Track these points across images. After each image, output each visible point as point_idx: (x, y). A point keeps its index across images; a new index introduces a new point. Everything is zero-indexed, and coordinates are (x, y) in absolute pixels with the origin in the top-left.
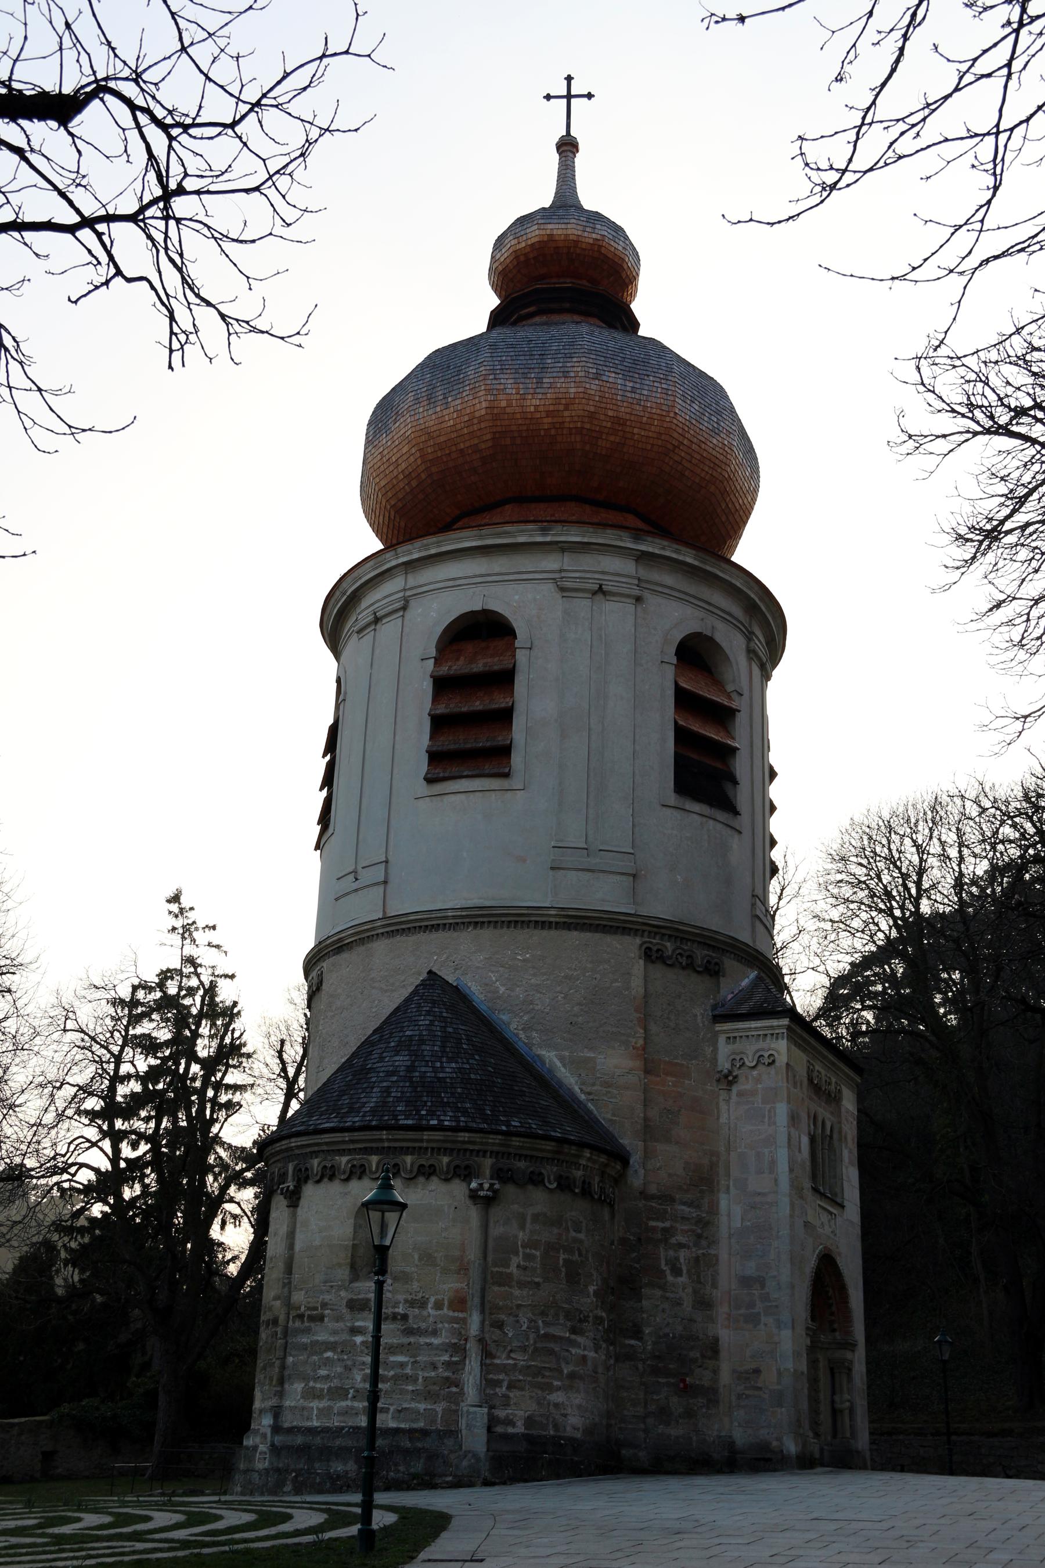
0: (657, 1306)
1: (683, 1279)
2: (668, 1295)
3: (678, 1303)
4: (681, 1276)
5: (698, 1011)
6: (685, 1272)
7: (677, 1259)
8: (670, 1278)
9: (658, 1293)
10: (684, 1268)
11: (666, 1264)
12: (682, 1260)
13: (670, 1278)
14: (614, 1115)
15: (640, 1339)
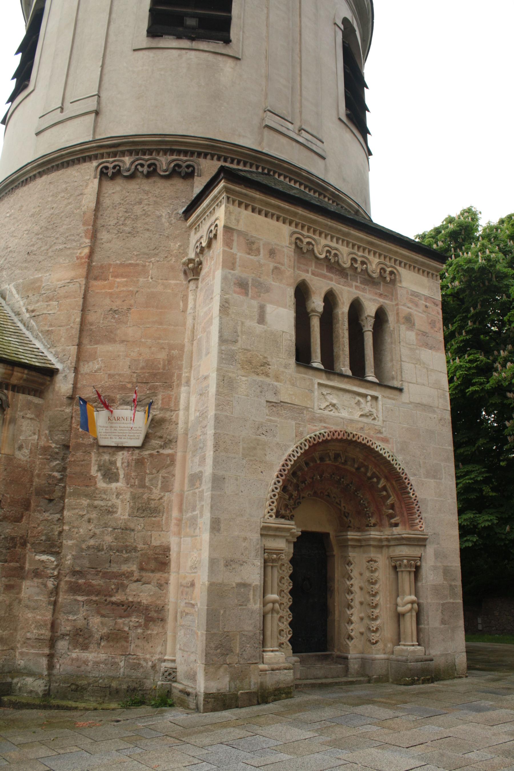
0: (82, 516)
1: (120, 484)
2: (96, 503)
3: (110, 511)
4: (117, 481)
5: (164, 212)
6: (122, 476)
7: (113, 463)
8: (101, 484)
9: (85, 502)
10: (121, 473)
11: (99, 470)
12: (119, 464)
13: (101, 484)
14: (51, 325)
15: (56, 554)
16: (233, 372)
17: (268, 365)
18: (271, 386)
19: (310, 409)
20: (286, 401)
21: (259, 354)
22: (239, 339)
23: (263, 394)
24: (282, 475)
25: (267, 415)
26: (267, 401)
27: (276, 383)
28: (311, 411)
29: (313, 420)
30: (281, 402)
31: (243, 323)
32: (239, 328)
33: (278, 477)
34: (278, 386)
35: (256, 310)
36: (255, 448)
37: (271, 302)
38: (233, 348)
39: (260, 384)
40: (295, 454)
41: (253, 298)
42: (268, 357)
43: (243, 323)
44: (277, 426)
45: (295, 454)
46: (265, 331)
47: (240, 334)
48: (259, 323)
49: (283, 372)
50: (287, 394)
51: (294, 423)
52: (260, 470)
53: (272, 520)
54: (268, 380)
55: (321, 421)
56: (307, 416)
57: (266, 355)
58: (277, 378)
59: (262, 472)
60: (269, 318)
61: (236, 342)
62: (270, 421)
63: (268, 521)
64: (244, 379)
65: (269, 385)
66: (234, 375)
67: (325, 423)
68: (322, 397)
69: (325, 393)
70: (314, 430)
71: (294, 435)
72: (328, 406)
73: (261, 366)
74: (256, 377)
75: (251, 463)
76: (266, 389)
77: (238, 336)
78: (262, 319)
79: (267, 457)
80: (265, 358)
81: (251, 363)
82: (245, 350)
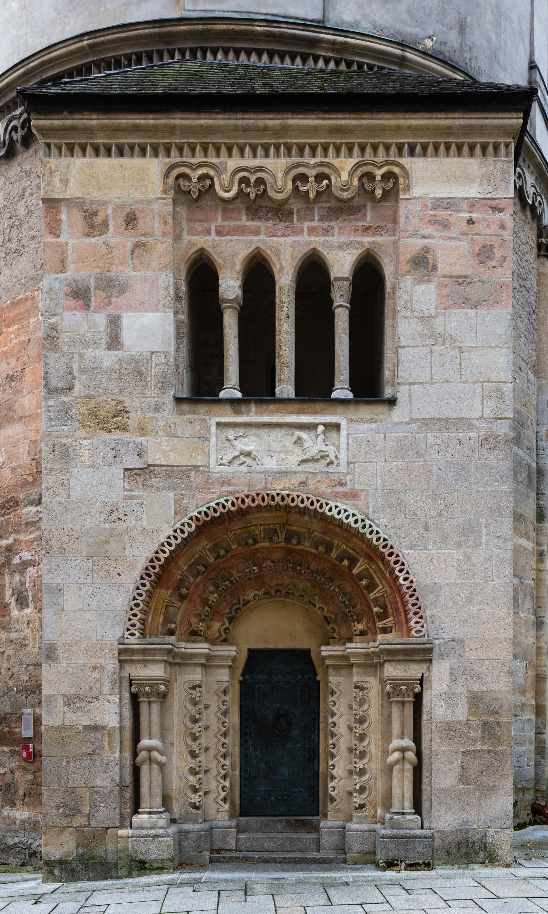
16: (68, 436)
17: (127, 412)
18: (132, 445)
19: (201, 469)
20: (158, 462)
21: (109, 400)
22: (76, 382)
23: (119, 459)
24: (149, 575)
25: (125, 490)
26: (126, 470)
27: (139, 439)
28: (204, 472)
29: (207, 485)
30: (150, 466)
31: (81, 356)
32: (75, 366)
33: (142, 578)
34: (145, 443)
35: (103, 328)
36: (107, 542)
37: (130, 308)
38: (67, 399)
39: (112, 446)
40: (173, 541)
41: (98, 310)
42: (126, 399)
43: (81, 356)
44: (142, 504)
45: (173, 541)
46: (120, 360)
47: (76, 374)
48: (109, 349)
49: (151, 418)
50: (161, 451)
51: (171, 494)
52: (116, 571)
53: (133, 640)
54: (125, 436)
55: (223, 484)
56: (195, 479)
57: (121, 398)
58: (142, 431)
59: (119, 574)
60: (127, 336)
61: (71, 388)
62: (131, 498)
63: (126, 641)
64: (86, 442)
65: (129, 443)
66: (70, 440)
67: (230, 485)
68: (227, 444)
69: (231, 437)
70: (201, 502)
71: (173, 513)
72: (236, 457)
73: (114, 416)
74: (105, 436)
75: (101, 564)
76: (123, 450)
77: (74, 378)
78: (114, 341)
79: (127, 553)
80: (120, 402)
81: (96, 416)
82: (86, 397)
